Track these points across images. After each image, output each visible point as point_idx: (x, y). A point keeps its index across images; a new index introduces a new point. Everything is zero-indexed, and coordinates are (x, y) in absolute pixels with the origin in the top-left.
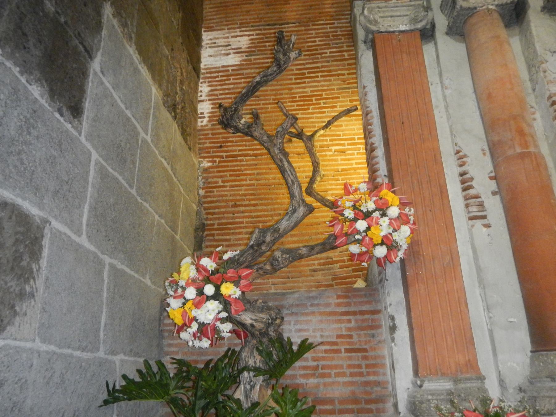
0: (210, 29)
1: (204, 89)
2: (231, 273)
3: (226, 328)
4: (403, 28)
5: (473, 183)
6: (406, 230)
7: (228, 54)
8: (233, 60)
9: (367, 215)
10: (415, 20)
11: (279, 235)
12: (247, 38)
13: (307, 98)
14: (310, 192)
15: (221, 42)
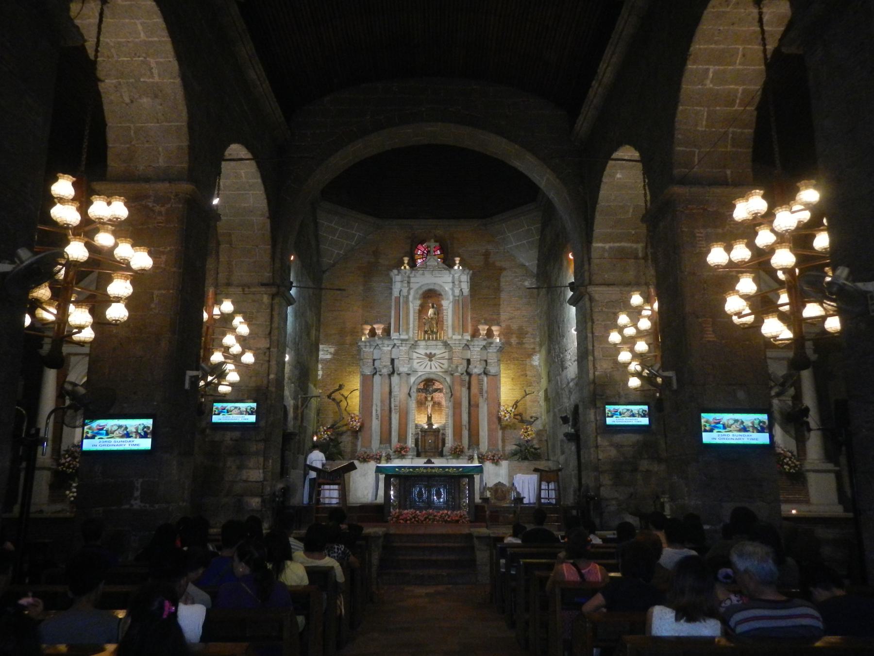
0: (322, 344)
1: (320, 366)
2: (329, 430)
3: (328, 439)
4: (369, 374)
5: (378, 412)
6: (359, 424)
7: (327, 354)
8: (329, 357)
9: (352, 421)
10: (371, 372)
11: (337, 423)
12: (333, 349)
13: (350, 372)
14: (345, 409)
15: (326, 349)
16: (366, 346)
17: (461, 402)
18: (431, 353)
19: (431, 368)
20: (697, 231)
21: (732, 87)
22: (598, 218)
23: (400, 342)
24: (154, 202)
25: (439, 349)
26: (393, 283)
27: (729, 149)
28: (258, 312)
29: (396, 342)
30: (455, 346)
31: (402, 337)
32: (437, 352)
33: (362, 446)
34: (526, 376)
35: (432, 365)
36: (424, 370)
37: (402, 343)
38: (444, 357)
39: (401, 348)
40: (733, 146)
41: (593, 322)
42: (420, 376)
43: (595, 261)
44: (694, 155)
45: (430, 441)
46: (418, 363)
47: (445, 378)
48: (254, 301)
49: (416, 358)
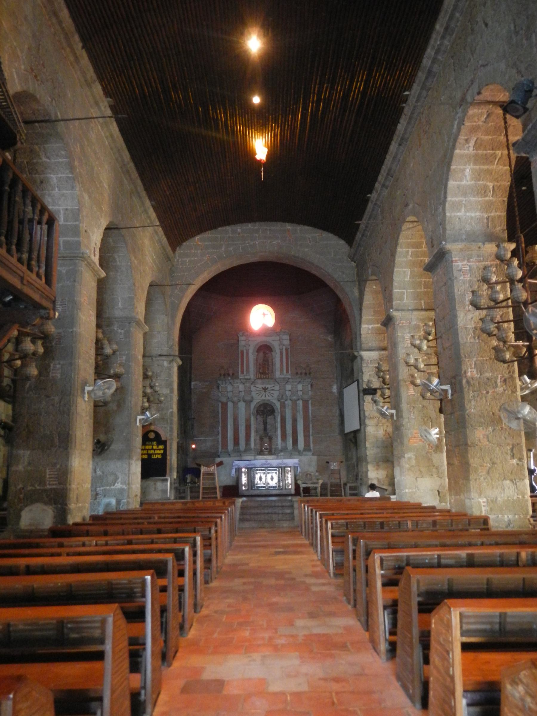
16: (222, 383)
19: (265, 396)
20: (405, 335)
21: (422, 258)
22: (364, 311)
24: (117, 327)
25: (270, 384)
27: (423, 290)
28: (161, 372)
29: (242, 380)
31: (246, 377)
32: (269, 386)
33: (222, 448)
40: (425, 288)
41: (363, 373)
42: (259, 402)
43: (363, 336)
44: (404, 294)
48: (158, 365)
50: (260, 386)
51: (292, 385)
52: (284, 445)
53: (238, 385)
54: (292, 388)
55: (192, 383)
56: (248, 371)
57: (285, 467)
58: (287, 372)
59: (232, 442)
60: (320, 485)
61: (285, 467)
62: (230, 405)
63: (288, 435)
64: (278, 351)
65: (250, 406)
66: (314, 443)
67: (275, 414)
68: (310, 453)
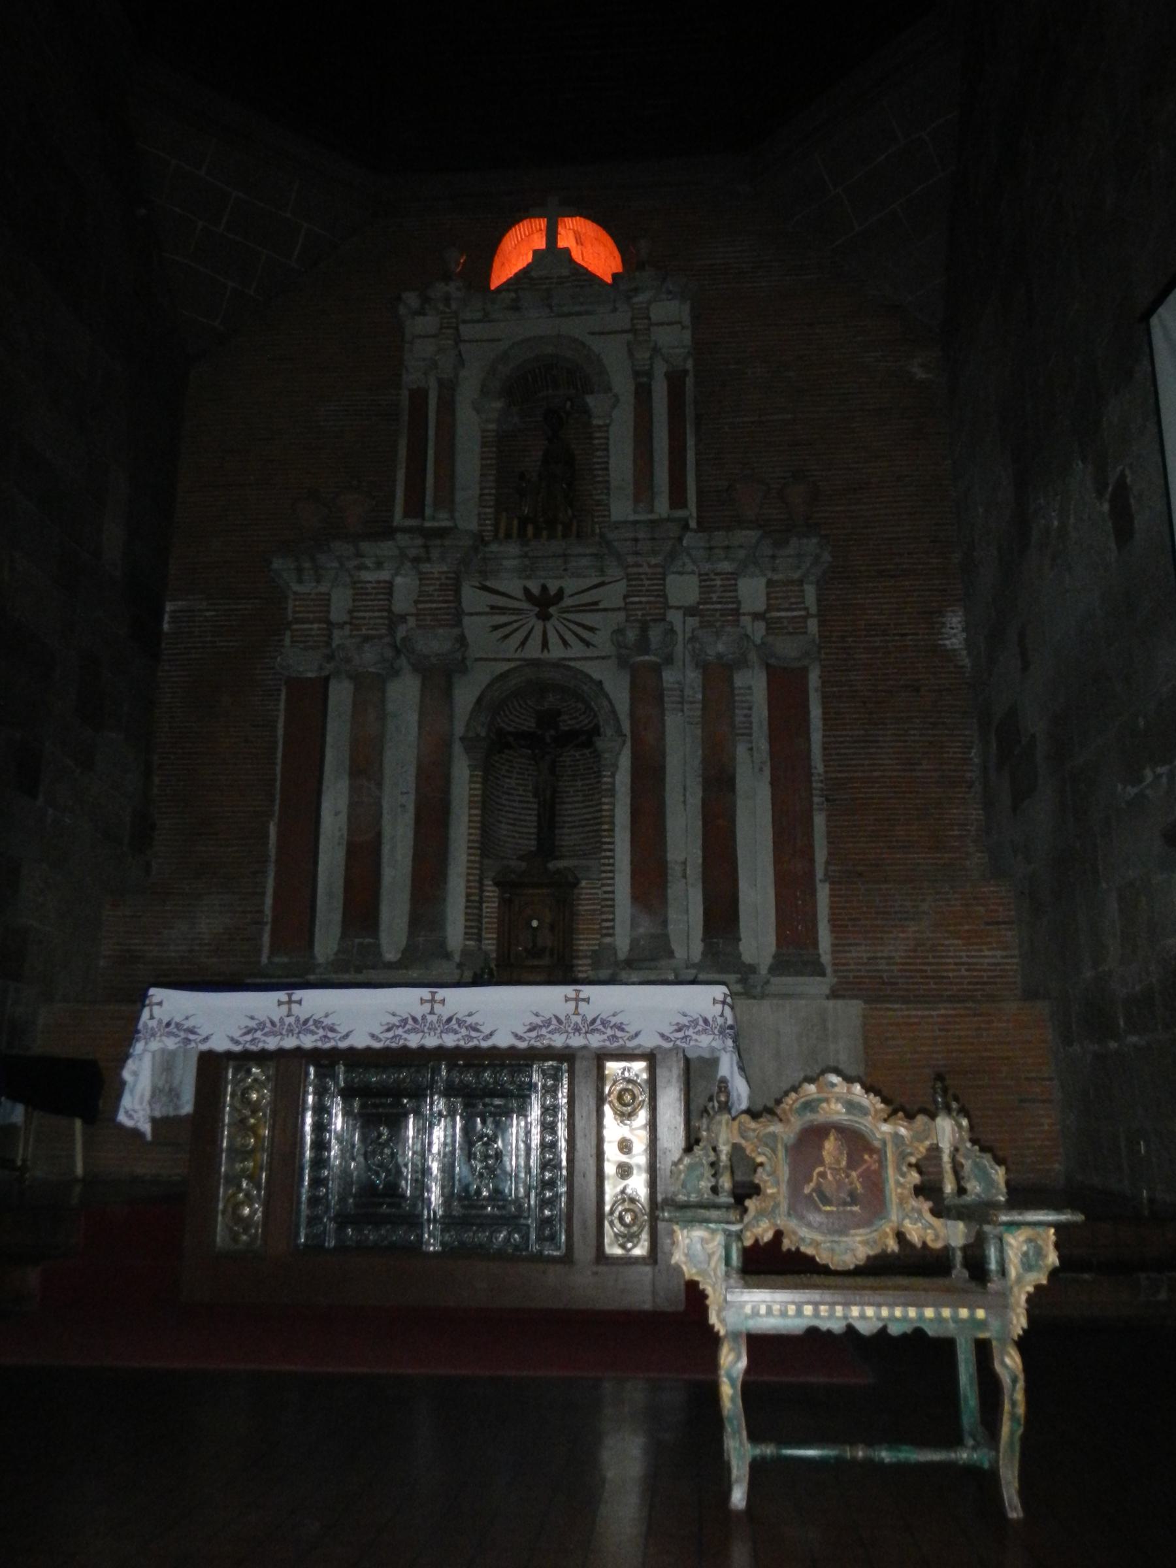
4: (310, 675)
17: (662, 768)
18: (544, 588)
19: (545, 645)
23: (419, 541)
26: (407, 345)
30: (637, 553)
34: (918, 690)
35: (553, 639)
36: (517, 656)
37: (426, 547)
38: (596, 603)
39: (425, 567)
42: (503, 676)
45: (535, 923)
46: (496, 628)
47: (600, 682)
49: (488, 610)
50: (513, 585)
51: (704, 577)
52: (646, 927)
53: (385, 575)
54: (706, 589)
55: (169, 607)
56: (446, 498)
57: (602, 1057)
58: (677, 498)
59: (337, 917)
60: (1019, 1322)
61: (602, 1057)
62: (340, 694)
63: (675, 871)
64: (622, 383)
65: (447, 694)
66: (837, 926)
67: (600, 744)
68: (817, 986)
